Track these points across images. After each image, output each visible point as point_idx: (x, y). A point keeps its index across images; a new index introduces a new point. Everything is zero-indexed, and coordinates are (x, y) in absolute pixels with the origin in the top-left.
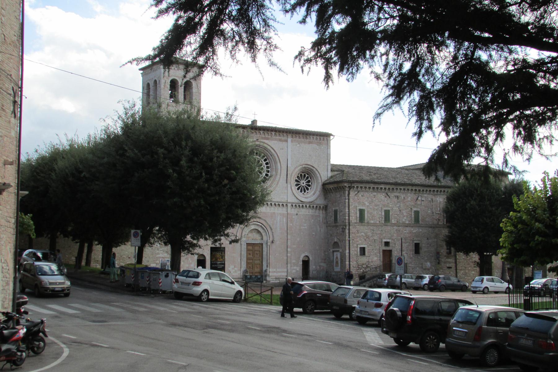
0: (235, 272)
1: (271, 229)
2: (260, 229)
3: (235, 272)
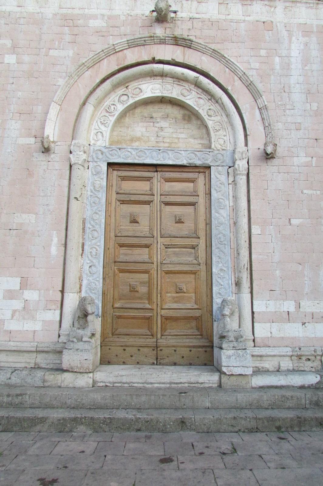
0: (27, 311)
1: (255, 94)
2: (192, 99)
3: (27, 311)
